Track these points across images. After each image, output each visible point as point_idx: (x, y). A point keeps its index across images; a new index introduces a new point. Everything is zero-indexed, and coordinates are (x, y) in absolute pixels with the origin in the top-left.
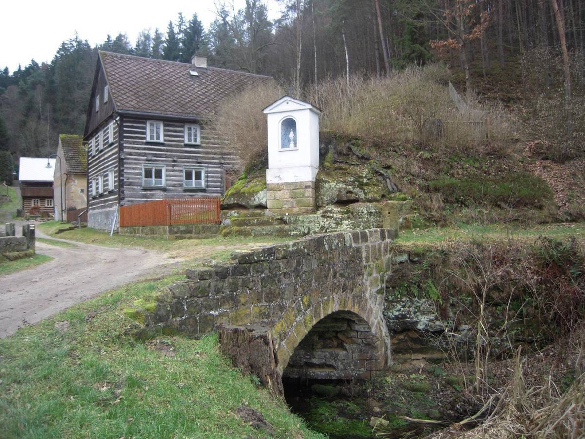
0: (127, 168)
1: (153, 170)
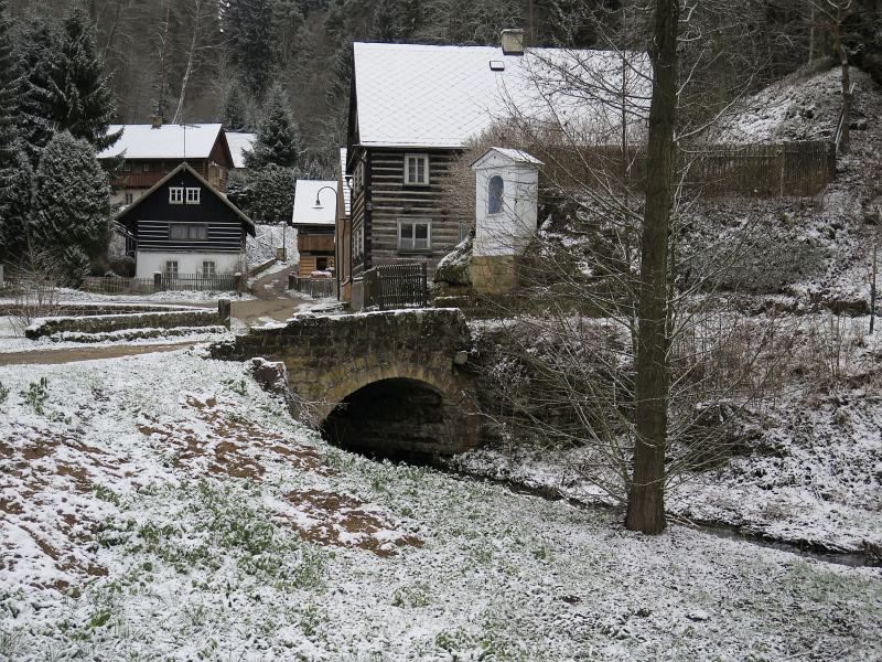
0: (375, 224)
1: (414, 227)
